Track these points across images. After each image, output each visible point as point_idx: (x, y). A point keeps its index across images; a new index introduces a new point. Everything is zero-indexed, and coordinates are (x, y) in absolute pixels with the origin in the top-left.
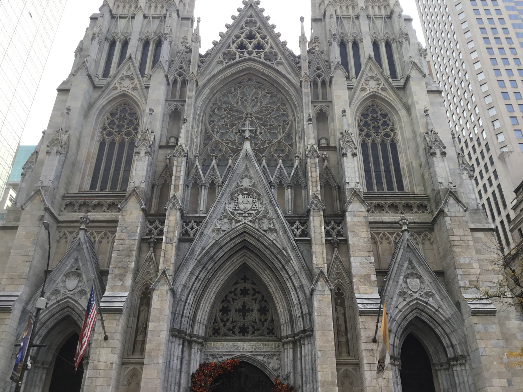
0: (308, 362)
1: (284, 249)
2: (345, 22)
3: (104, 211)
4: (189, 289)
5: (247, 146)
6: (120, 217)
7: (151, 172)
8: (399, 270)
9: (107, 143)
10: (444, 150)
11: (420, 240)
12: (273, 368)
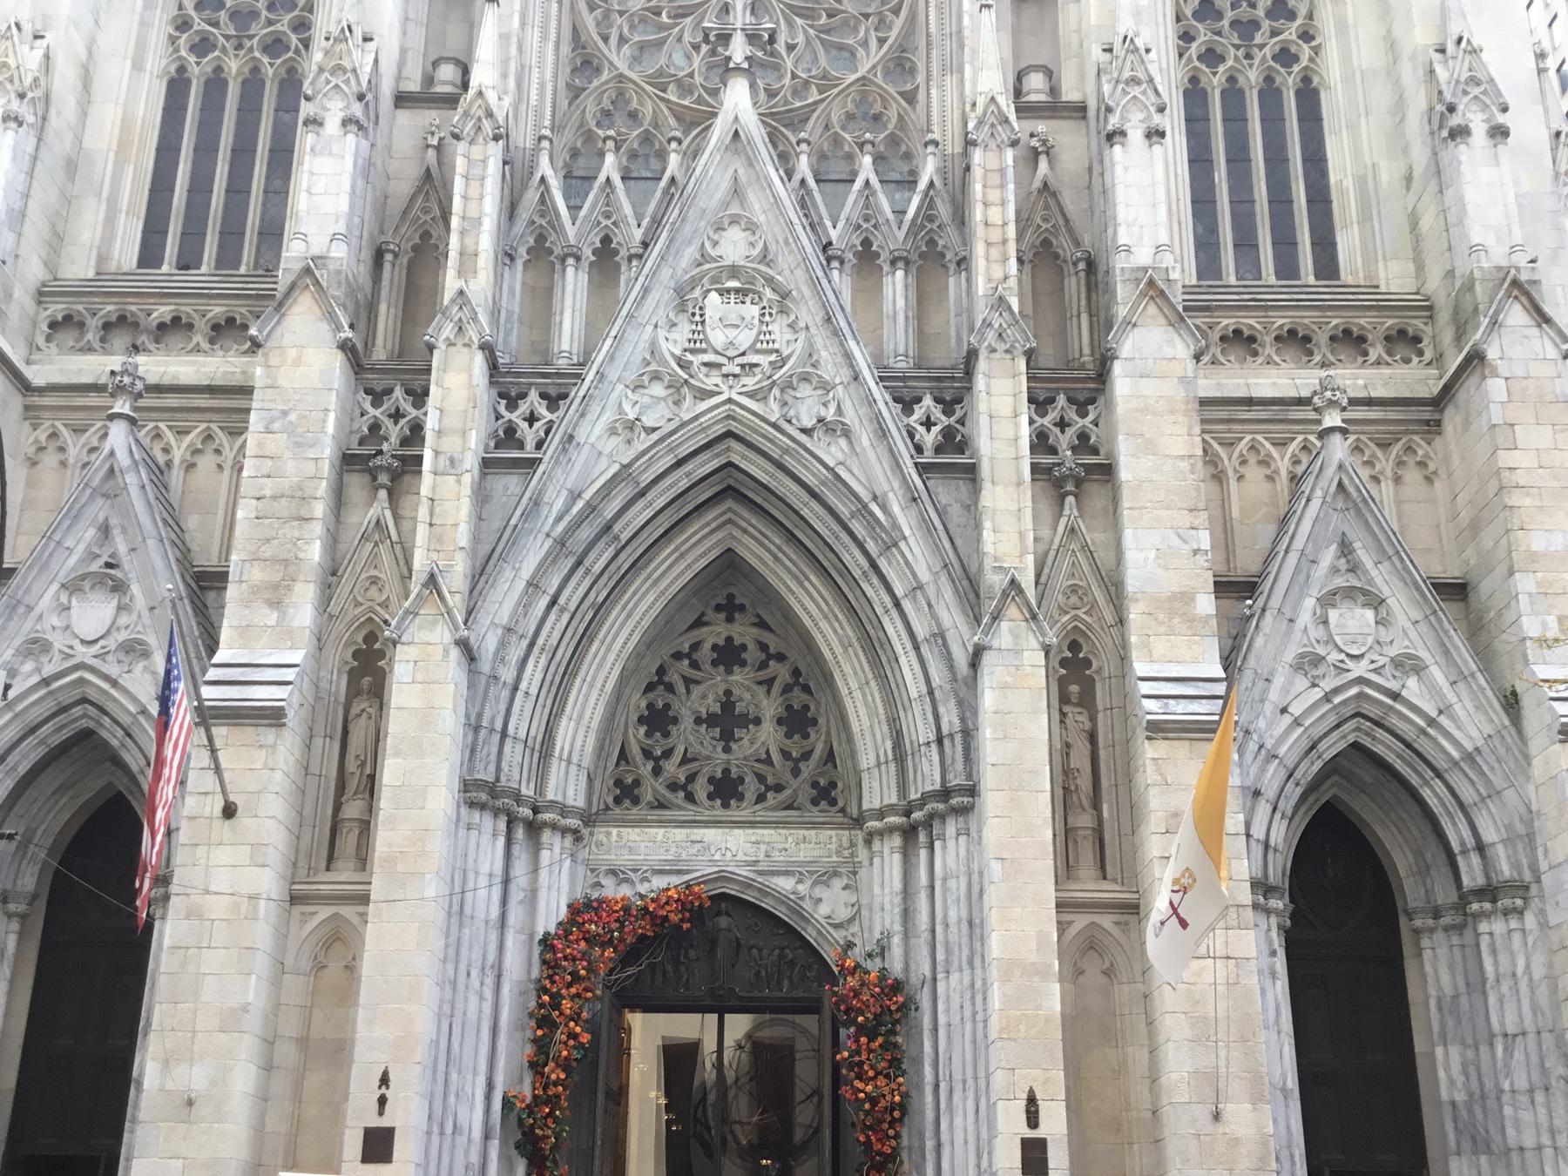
0: (954, 897)
1: (875, 498)
3: (197, 350)
4: (525, 643)
5: (738, 100)
6: (259, 371)
7: (369, 199)
8: (1302, 577)
9: (194, 83)
10: (1501, 119)
11: (1385, 463)
12: (829, 917)
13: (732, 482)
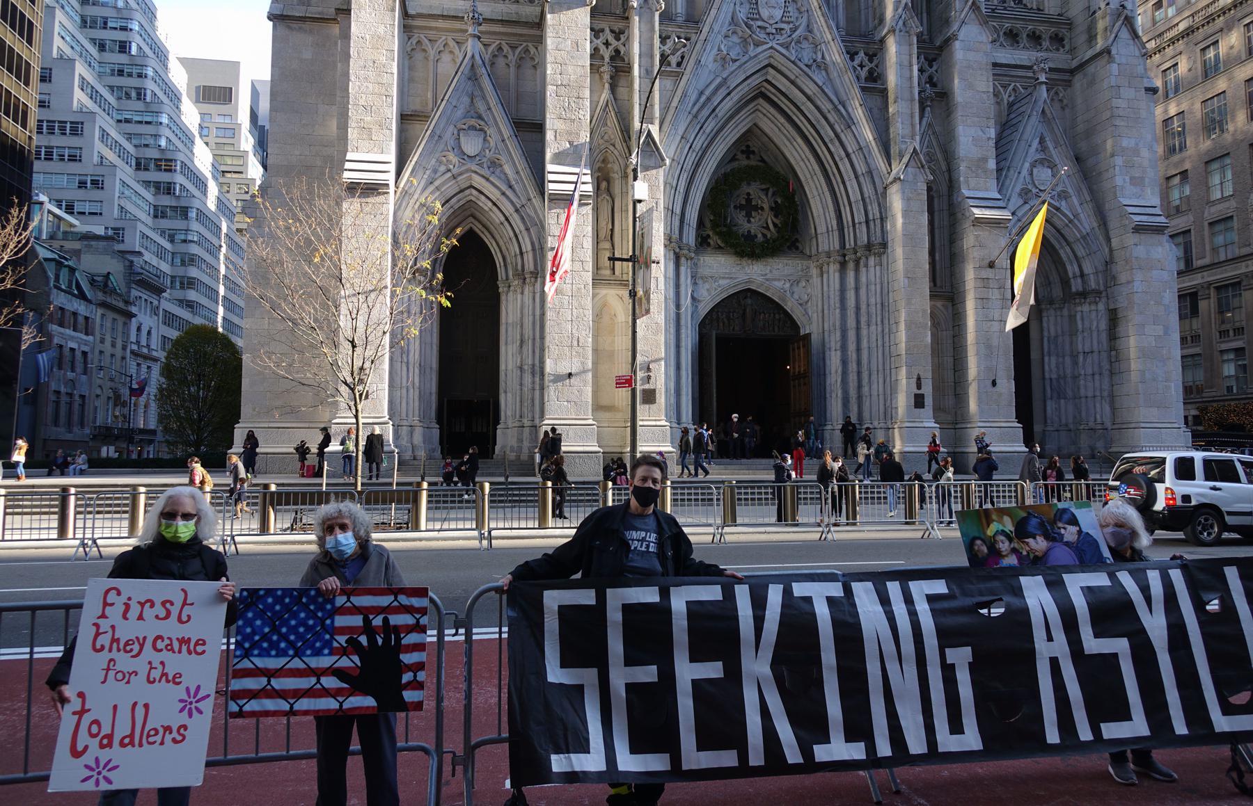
0: (873, 292)
13: (763, 89)
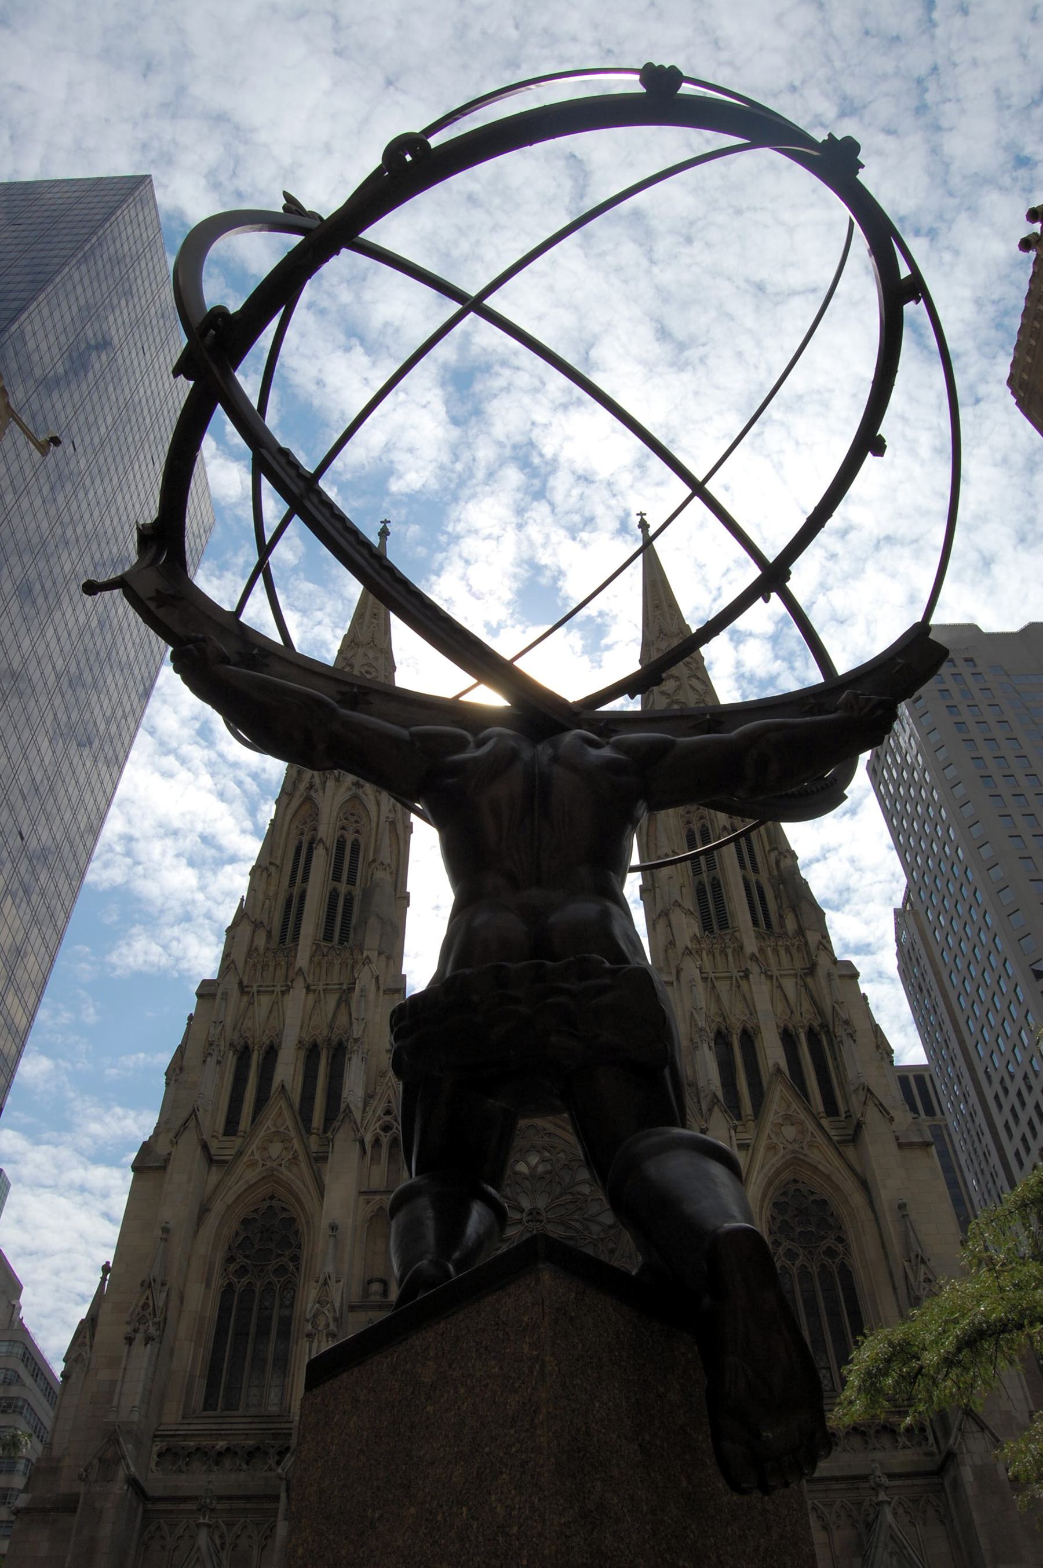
2: (723, 987)
